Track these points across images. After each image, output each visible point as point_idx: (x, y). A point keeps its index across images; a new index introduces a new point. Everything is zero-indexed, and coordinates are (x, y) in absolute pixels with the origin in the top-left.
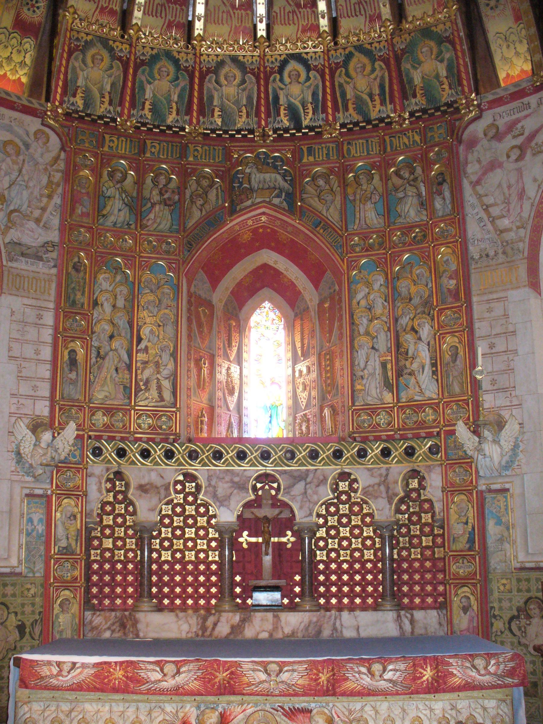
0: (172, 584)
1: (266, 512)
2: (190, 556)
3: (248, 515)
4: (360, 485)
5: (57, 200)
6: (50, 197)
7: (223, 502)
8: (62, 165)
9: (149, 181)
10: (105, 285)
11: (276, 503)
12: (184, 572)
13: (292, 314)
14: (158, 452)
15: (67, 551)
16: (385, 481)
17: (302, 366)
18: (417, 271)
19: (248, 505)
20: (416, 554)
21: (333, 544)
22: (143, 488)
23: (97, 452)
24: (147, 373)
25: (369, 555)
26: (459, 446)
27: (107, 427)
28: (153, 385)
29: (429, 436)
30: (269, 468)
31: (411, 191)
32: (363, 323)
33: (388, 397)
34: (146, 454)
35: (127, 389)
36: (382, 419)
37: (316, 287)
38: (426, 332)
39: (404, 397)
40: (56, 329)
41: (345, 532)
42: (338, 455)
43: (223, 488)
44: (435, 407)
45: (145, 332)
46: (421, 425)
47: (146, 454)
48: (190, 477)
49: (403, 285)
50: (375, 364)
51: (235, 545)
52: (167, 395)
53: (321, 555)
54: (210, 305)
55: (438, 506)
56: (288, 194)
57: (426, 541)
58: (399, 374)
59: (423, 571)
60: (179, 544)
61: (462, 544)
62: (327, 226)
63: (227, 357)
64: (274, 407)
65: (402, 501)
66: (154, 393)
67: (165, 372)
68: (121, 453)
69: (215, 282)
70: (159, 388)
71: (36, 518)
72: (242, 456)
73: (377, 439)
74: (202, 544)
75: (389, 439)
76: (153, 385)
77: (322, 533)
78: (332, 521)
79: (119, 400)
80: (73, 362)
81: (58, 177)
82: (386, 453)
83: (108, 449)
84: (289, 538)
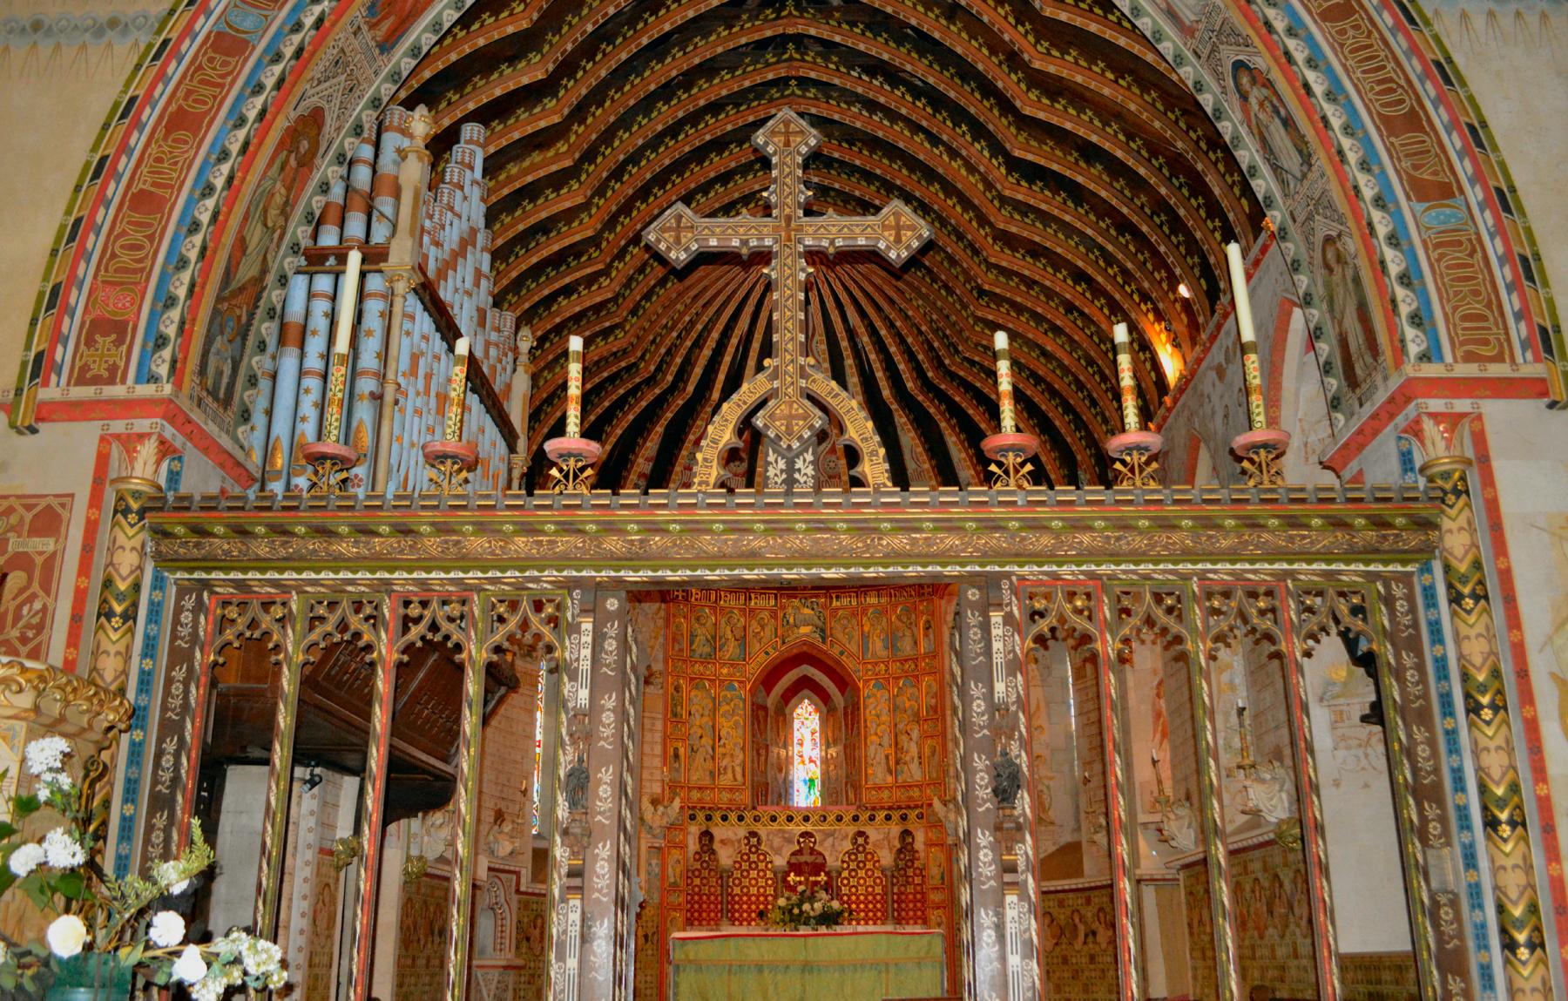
0: (741, 911)
1: (806, 858)
2: (754, 890)
3: (793, 860)
4: (871, 840)
5: (661, 640)
6: (656, 638)
7: (778, 851)
8: (662, 613)
9: (723, 621)
10: (695, 700)
11: (812, 852)
12: (749, 903)
13: (825, 710)
14: (733, 817)
15: (675, 884)
16: (887, 837)
17: (833, 751)
18: (911, 690)
19: (793, 854)
20: (910, 889)
21: (853, 882)
22: (723, 842)
23: (693, 817)
24: (724, 763)
25: (878, 890)
26: (934, 814)
27: (700, 800)
28: (729, 771)
29: (917, 807)
30: (809, 827)
31: (908, 633)
32: (872, 728)
33: (890, 779)
34: (725, 818)
35: (712, 774)
36: (885, 794)
37: (843, 693)
38: (915, 734)
39: (900, 780)
40: (665, 733)
41: (861, 873)
42: (856, 818)
43: (777, 842)
44: (919, 786)
45: (723, 733)
46: (910, 798)
47: (725, 818)
48: (753, 834)
49: (899, 700)
50: (881, 756)
51: (785, 881)
52: (739, 777)
53: (845, 890)
54: (765, 708)
55: (922, 855)
56: (823, 630)
57: (918, 880)
58: (897, 762)
59: (915, 901)
60: (746, 882)
61: (936, 882)
62: (851, 655)
63: (777, 745)
64: (812, 780)
65: (900, 851)
66: (730, 775)
67: (738, 761)
68: (709, 818)
69: (768, 692)
70: (734, 771)
71: (654, 862)
72: (790, 819)
73: (882, 808)
74: (762, 882)
75: (890, 808)
76: (729, 771)
77: (845, 874)
78: (853, 865)
79: (707, 782)
80: (676, 756)
81: (661, 623)
82: (888, 818)
83: (701, 816)
84: (822, 878)
